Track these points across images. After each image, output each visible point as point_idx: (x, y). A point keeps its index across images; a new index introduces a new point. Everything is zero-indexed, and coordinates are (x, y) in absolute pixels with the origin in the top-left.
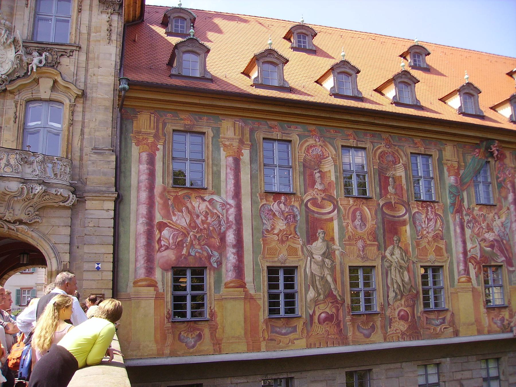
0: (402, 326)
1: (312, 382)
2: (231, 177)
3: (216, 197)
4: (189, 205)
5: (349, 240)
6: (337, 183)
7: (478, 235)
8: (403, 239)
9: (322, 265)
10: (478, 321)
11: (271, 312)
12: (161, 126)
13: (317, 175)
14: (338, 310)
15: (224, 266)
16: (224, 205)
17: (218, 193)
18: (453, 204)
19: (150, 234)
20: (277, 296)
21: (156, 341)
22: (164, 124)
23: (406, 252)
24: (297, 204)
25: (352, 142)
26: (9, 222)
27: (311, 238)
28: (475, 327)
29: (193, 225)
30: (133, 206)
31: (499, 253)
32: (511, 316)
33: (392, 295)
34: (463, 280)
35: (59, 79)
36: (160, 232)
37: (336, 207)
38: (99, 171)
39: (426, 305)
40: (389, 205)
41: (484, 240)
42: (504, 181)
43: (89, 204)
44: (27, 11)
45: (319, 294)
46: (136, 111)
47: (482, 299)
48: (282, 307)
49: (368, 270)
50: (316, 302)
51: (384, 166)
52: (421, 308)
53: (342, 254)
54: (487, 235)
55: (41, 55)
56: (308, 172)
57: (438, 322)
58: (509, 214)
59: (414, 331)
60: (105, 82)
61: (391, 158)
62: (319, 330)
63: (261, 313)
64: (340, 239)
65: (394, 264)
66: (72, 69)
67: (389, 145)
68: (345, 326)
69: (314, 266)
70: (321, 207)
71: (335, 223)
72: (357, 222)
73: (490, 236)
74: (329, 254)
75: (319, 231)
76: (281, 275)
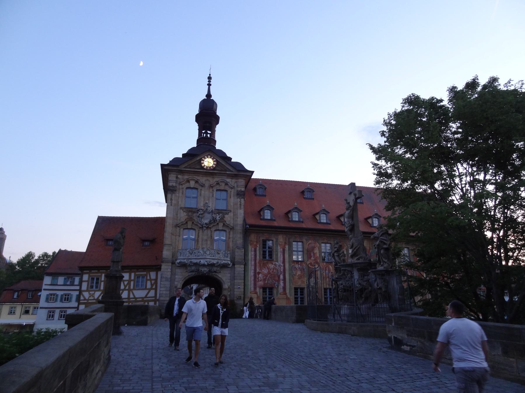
3: (276, 263)
16: (280, 266)
17: (277, 261)
20: (297, 298)
22: (259, 238)
24: (305, 265)
29: (269, 273)
30: (250, 267)
37: (319, 266)
38: (239, 254)
43: (236, 266)
76: (299, 290)
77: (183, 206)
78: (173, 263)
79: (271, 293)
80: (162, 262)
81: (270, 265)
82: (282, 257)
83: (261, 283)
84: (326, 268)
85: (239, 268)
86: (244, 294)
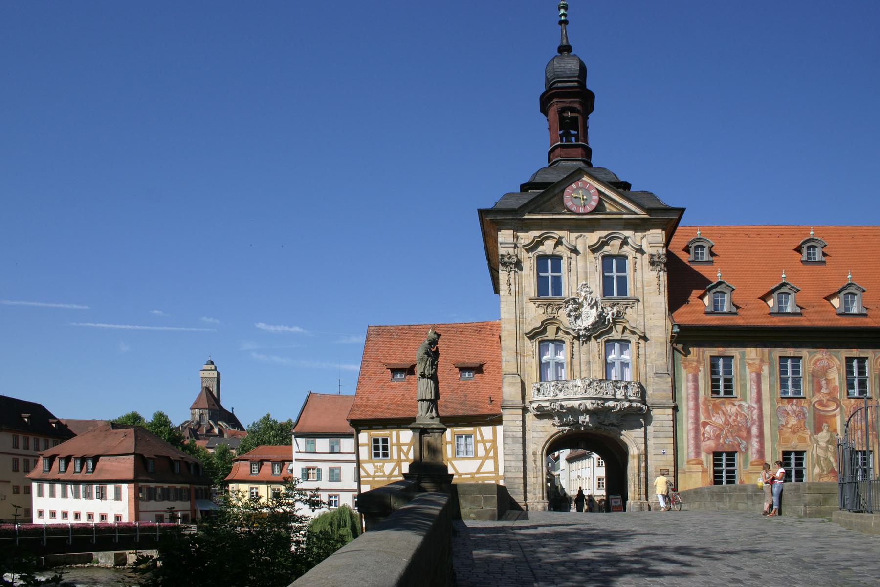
3: (743, 403)
4: (723, 409)
6: (840, 387)
12: (701, 353)
17: (745, 400)
19: (697, 430)
24: (806, 405)
27: (818, 429)
29: (727, 423)
35: (627, 326)
37: (839, 405)
56: (816, 380)
66: (635, 316)
70: (826, 406)
71: (838, 418)
75: (825, 424)
82: (754, 391)
83: (711, 444)
85: (661, 417)
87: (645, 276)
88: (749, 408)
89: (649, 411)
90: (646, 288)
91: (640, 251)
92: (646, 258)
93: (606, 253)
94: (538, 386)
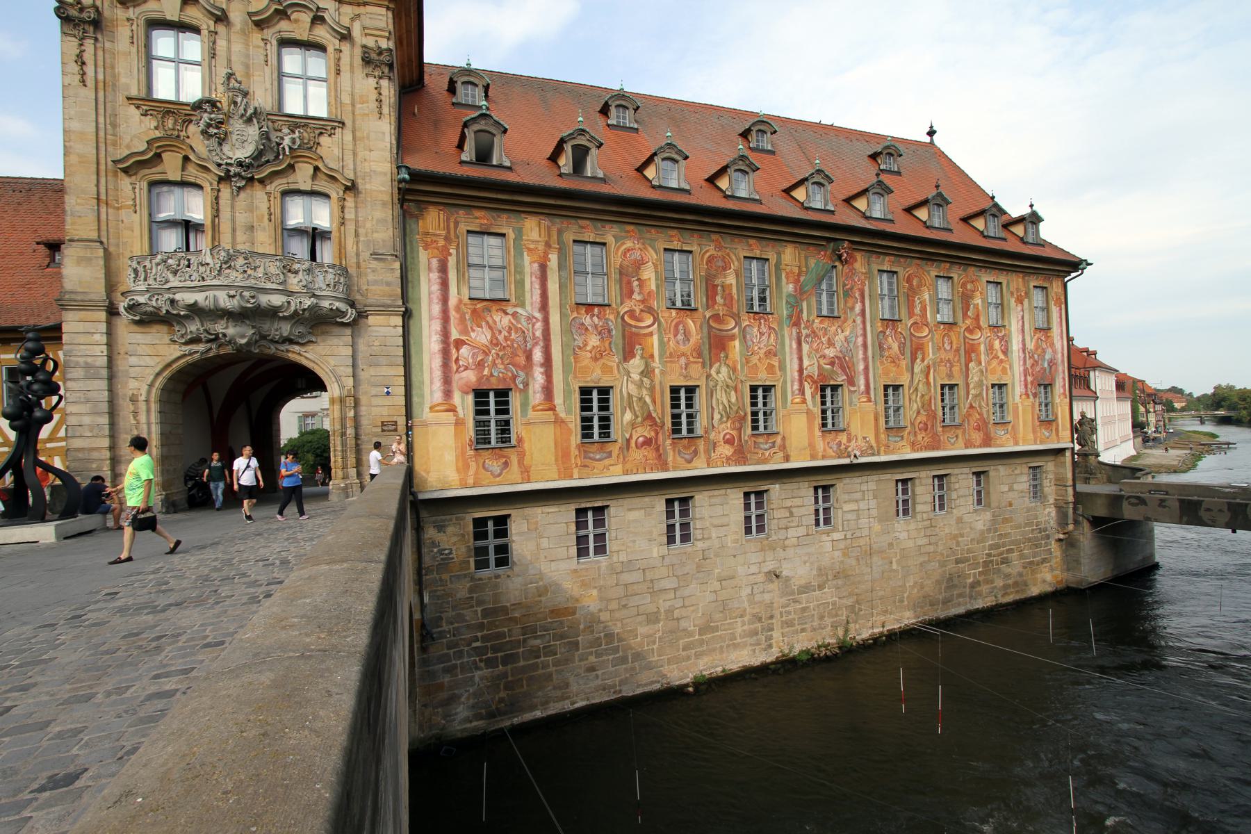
0: (727, 450)
1: (630, 510)
2: (537, 286)
3: (520, 310)
4: (489, 319)
5: (670, 357)
7: (817, 350)
8: (731, 356)
9: (640, 385)
10: (812, 445)
11: (584, 436)
12: (452, 225)
13: (636, 283)
14: (657, 434)
15: (531, 387)
17: (523, 305)
18: (790, 316)
19: (445, 353)
20: (590, 419)
21: (458, 470)
22: (457, 224)
23: (734, 370)
24: (612, 317)
25: (676, 245)
26: (277, 342)
27: (628, 355)
28: (808, 452)
29: (494, 342)
30: (425, 322)
31: (839, 371)
32: (849, 440)
33: (717, 417)
34: (797, 400)
35: (321, 166)
36: (458, 350)
37: (656, 319)
39: (755, 428)
40: (716, 317)
41: (824, 357)
42: (852, 289)
44: (267, 70)
45: (637, 417)
46: (422, 206)
47: (819, 421)
48: (596, 430)
49: (691, 390)
50: (633, 425)
51: (713, 272)
52: (749, 431)
53: (663, 373)
54: (827, 352)
55: (294, 132)
57: (767, 446)
58: (855, 327)
59: (741, 455)
60: (379, 169)
61: (720, 264)
62: (636, 455)
63: (573, 438)
64: (661, 356)
65: (720, 384)
66: (336, 151)
67: (720, 248)
68: (665, 450)
69: (631, 386)
71: (655, 337)
72: (680, 337)
73: (831, 353)
74: (647, 372)
77: (134, 92)
78: (112, 312)
79: (503, 408)
80: (63, 307)
81: (497, 319)
82: (537, 292)
84: (677, 326)
86: (409, 415)
87: (357, 86)
88: (528, 319)
89: (362, 315)
90: (358, 106)
91: (346, 37)
92: (358, 52)
93: (286, 35)
94: (135, 265)
